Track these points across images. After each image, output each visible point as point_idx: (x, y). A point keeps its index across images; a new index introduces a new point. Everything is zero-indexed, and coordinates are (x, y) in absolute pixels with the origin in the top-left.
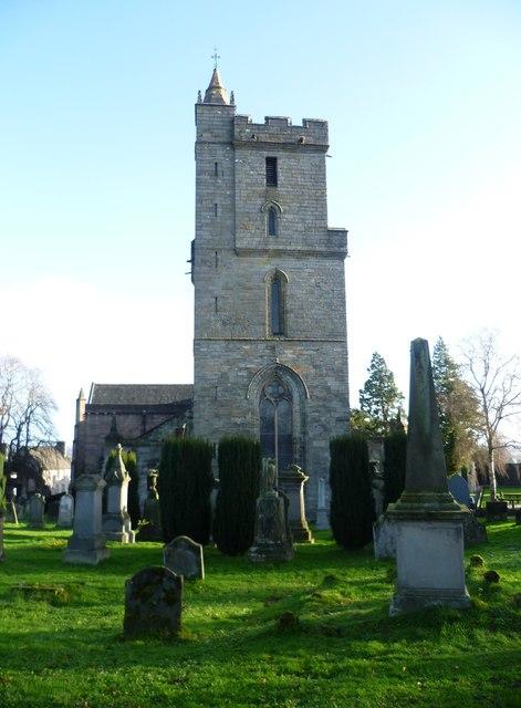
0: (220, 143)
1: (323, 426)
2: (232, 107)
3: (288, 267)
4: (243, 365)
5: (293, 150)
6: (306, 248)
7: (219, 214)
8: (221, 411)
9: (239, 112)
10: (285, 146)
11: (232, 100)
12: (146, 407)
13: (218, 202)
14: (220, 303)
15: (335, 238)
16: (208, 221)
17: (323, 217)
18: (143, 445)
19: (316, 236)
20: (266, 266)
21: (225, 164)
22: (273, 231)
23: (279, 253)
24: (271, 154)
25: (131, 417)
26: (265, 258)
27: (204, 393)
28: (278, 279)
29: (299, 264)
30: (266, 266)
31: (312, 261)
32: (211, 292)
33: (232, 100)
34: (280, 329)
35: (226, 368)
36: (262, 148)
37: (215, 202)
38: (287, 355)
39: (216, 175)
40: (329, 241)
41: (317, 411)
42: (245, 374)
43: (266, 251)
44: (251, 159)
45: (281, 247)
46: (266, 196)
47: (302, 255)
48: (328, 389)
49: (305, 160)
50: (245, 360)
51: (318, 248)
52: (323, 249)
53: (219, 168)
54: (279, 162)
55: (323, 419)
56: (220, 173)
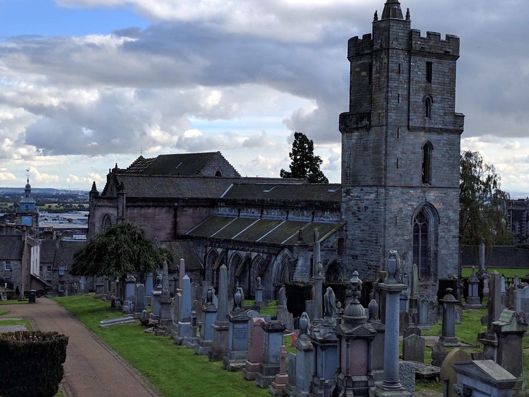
0: (402, 49)
1: (446, 241)
2: (408, 21)
3: (434, 137)
4: (409, 203)
5: (441, 58)
6: (443, 127)
7: (400, 102)
8: (399, 232)
10: (439, 56)
11: (408, 13)
12: (177, 200)
13: (400, 93)
14: (399, 163)
15: (459, 120)
17: (453, 106)
19: (449, 119)
20: (423, 138)
22: (428, 114)
23: (430, 130)
24: (429, 60)
25: (164, 210)
26: (422, 133)
27: (391, 221)
28: (427, 147)
30: (423, 138)
32: (396, 155)
33: (408, 16)
34: (426, 179)
35: (401, 206)
36: (424, 56)
37: (399, 93)
38: (432, 196)
39: (399, 73)
40: (455, 123)
41: (443, 232)
42: (410, 209)
44: (419, 63)
45: (432, 126)
46: (426, 90)
47: (441, 131)
48: (449, 218)
49: (446, 62)
50: (411, 200)
52: (452, 128)
53: (401, 69)
54: (433, 66)
55: (446, 236)
56: (401, 72)
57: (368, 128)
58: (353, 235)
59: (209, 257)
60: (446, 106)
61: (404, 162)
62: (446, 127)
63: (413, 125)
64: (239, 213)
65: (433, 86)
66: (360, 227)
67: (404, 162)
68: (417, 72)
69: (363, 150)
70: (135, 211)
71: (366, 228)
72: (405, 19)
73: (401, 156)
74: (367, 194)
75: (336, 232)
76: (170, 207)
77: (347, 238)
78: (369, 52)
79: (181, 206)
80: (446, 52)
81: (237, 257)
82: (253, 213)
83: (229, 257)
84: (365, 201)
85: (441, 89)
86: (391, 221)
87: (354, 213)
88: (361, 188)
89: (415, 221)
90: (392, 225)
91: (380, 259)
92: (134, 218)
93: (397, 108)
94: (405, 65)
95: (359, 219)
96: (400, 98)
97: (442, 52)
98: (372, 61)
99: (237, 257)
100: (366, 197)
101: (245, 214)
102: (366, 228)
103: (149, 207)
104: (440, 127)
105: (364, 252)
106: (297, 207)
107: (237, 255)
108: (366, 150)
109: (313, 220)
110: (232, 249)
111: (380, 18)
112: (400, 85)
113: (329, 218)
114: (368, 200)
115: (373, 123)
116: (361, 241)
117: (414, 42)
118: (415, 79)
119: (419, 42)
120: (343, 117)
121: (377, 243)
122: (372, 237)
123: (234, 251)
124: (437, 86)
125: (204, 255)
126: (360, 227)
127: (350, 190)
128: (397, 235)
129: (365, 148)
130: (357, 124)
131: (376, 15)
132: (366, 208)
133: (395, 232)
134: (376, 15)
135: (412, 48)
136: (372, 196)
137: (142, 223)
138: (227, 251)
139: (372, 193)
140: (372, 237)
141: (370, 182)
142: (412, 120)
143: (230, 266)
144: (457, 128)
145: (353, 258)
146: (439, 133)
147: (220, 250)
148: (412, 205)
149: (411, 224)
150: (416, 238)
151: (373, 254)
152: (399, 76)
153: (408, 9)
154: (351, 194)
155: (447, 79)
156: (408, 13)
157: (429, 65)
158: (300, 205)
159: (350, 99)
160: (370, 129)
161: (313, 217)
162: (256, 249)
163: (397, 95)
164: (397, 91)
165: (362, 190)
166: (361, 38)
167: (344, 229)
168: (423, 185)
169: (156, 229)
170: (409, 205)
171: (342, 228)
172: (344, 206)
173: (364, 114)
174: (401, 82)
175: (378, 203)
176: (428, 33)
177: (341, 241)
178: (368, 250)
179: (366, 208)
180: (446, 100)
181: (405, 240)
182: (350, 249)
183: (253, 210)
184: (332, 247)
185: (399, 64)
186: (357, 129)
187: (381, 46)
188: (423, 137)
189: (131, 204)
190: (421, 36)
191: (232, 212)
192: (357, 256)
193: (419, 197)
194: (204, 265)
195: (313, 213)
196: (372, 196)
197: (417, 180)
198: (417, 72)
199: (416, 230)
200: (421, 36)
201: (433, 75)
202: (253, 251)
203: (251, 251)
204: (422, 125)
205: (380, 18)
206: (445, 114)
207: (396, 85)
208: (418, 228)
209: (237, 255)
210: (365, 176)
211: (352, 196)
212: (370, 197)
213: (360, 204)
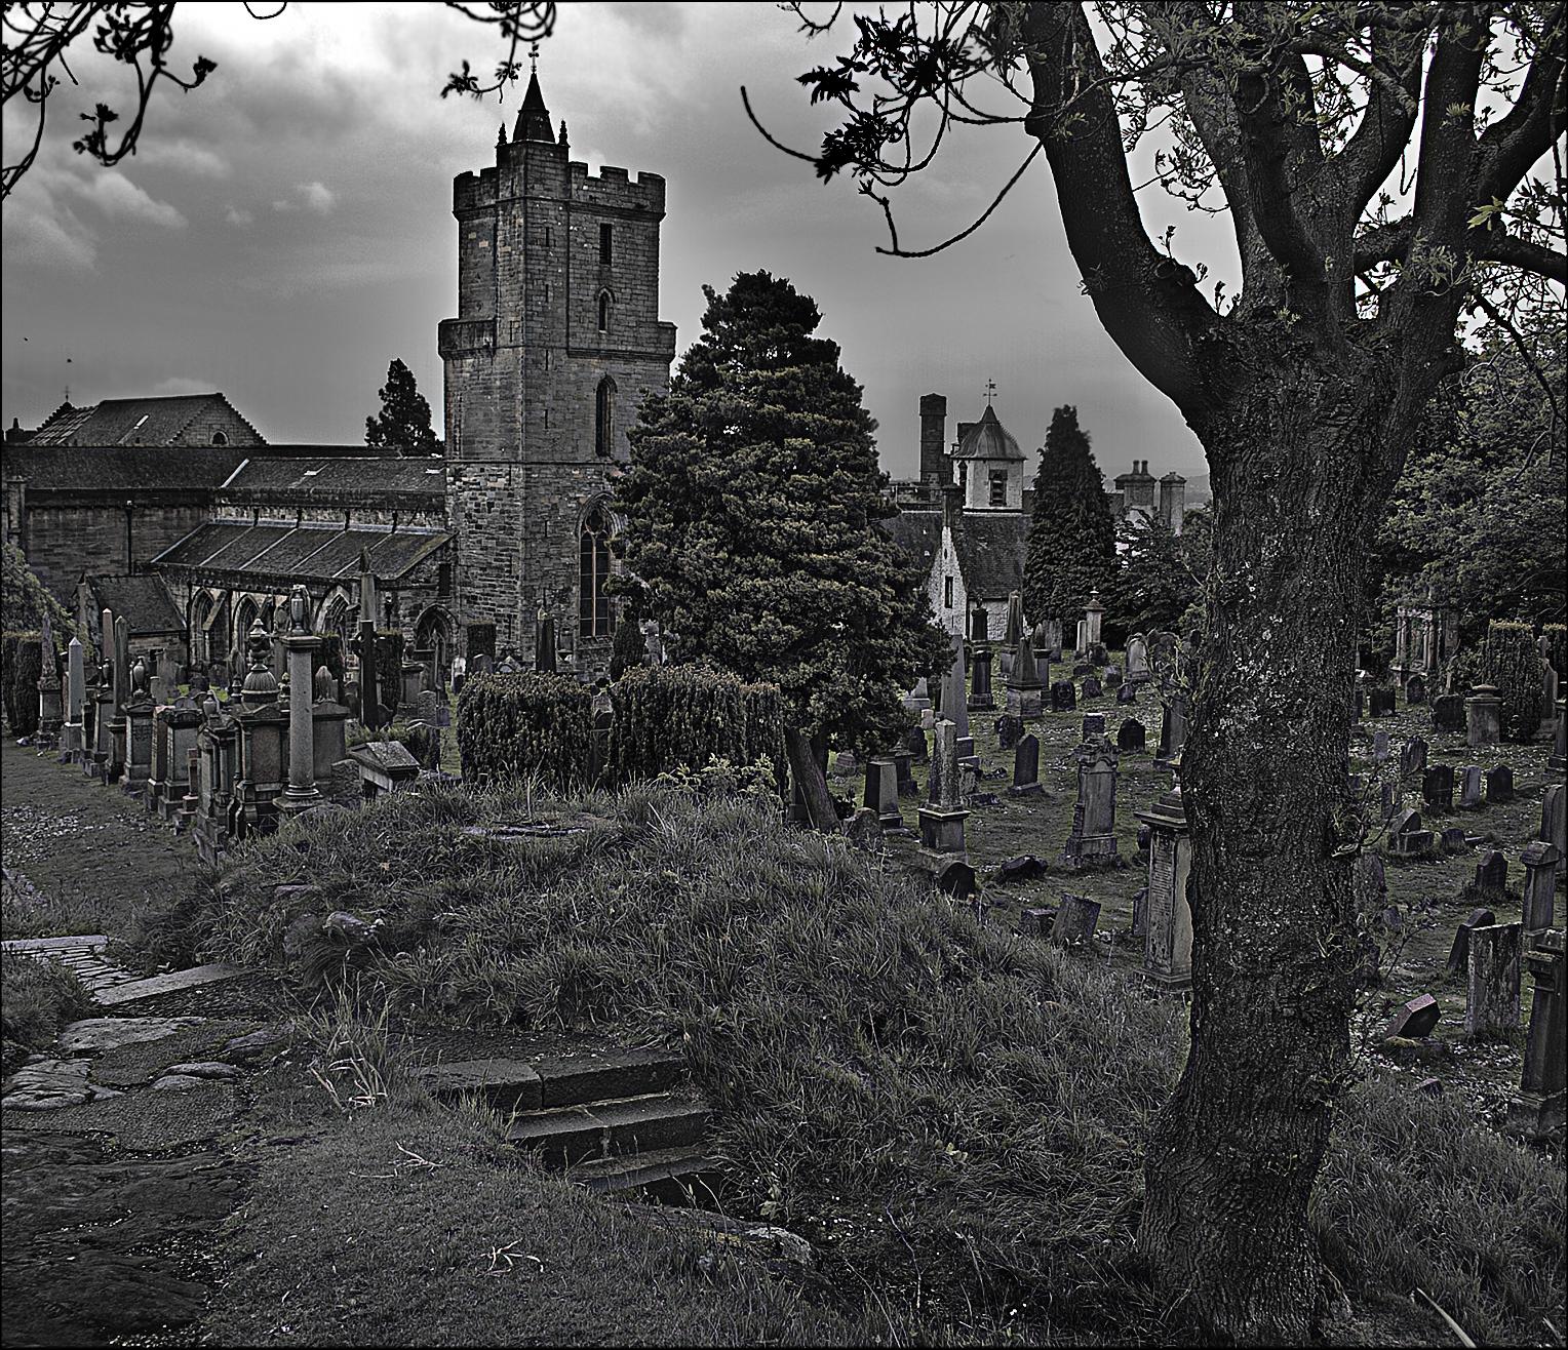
2: (563, 148)
3: (618, 367)
4: (571, 495)
7: (550, 300)
9: (573, 157)
11: (563, 130)
12: (131, 494)
15: (665, 337)
16: (539, 309)
18: (404, 588)
20: (597, 370)
21: (559, 229)
23: (610, 355)
26: (595, 361)
28: (605, 386)
29: (627, 368)
30: (597, 370)
31: (639, 366)
33: (563, 136)
35: (556, 500)
43: (599, 351)
45: (612, 347)
47: (630, 357)
51: (649, 350)
53: (551, 236)
54: (613, 232)
56: (552, 243)
57: (491, 351)
58: (469, 557)
59: (196, 606)
60: (640, 308)
61: (559, 416)
62: (639, 349)
63: (577, 345)
64: (257, 517)
65: (614, 270)
66: (480, 542)
67: (559, 416)
68: (582, 244)
69: (484, 393)
70: (46, 518)
71: (491, 543)
72: (557, 141)
73: (553, 405)
74: (491, 478)
75: (434, 552)
76: (117, 508)
77: (456, 563)
78: (493, 202)
79: (139, 505)
80: (639, 206)
81: (249, 604)
82: (283, 517)
83: (233, 605)
84: (489, 493)
85: (632, 277)
86: (536, 529)
87: (468, 516)
88: (481, 466)
89: (583, 528)
90: (538, 536)
91: (517, 603)
92: (43, 530)
93: (544, 313)
94: (559, 229)
95: (479, 527)
96: (550, 294)
97: (630, 206)
98: (497, 221)
99: (249, 604)
100: (490, 484)
101: (269, 520)
102: (491, 543)
103: (74, 508)
104: (629, 348)
105: (488, 590)
106: (365, 504)
107: (248, 601)
108: (488, 394)
109: (394, 529)
110: (239, 590)
111: (510, 140)
112: (550, 269)
113: (423, 525)
114: (493, 489)
115: (500, 342)
116: (481, 569)
117: (575, 186)
118: (578, 256)
119: (585, 188)
120: (446, 327)
121: (510, 572)
122: (502, 561)
123: (242, 594)
124: (623, 270)
125: (187, 601)
126: (480, 542)
127: (460, 469)
128: (547, 556)
129: (488, 390)
130: (472, 342)
131: (502, 131)
132: (490, 505)
133: (545, 550)
134: (502, 131)
135: (571, 197)
136: (502, 481)
137: (61, 542)
138: (230, 595)
139: (500, 476)
140: (502, 561)
141: (497, 456)
142: (574, 334)
143: (236, 622)
144: (663, 351)
145: (468, 602)
146: (627, 362)
147: (216, 593)
148: (576, 498)
149: (576, 535)
150: (586, 562)
151: (504, 592)
152: (547, 252)
153: (563, 123)
154: (464, 479)
155: (640, 258)
156: (563, 130)
157: (606, 230)
158: (370, 501)
159: (460, 293)
160: (494, 353)
161: (395, 525)
162: (283, 589)
163: (543, 288)
164: (544, 280)
165: (482, 470)
166: (477, 174)
167: (452, 545)
168: (598, 461)
169: (89, 553)
170: (570, 499)
171: (446, 543)
172: (451, 500)
173: (483, 322)
174: (551, 262)
175: (510, 495)
176: (603, 169)
177: (444, 569)
178: (494, 586)
179: (490, 505)
180: (640, 297)
181: (564, 564)
182: (466, 584)
183: (282, 512)
184: (427, 581)
185: (548, 228)
186: (472, 352)
187: (513, 194)
188: (596, 367)
189: (36, 504)
190: (591, 174)
191: (242, 516)
192: (475, 598)
193: (590, 484)
194: (188, 623)
195: (395, 516)
196: (502, 481)
197: (587, 451)
198: (582, 244)
199: (586, 545)
200: (591, 174)
201: (613, 250)
202: (279, 592)
203: (275, 593)
204: (593, 346)
205: (510, 140)
206: (639, 324)
207: (542, 268)
208: (591, 542)
209: (248, 601)
210: (488, 442)
211: (465, 483)
212: (496, 485)
213: (480, 498)
